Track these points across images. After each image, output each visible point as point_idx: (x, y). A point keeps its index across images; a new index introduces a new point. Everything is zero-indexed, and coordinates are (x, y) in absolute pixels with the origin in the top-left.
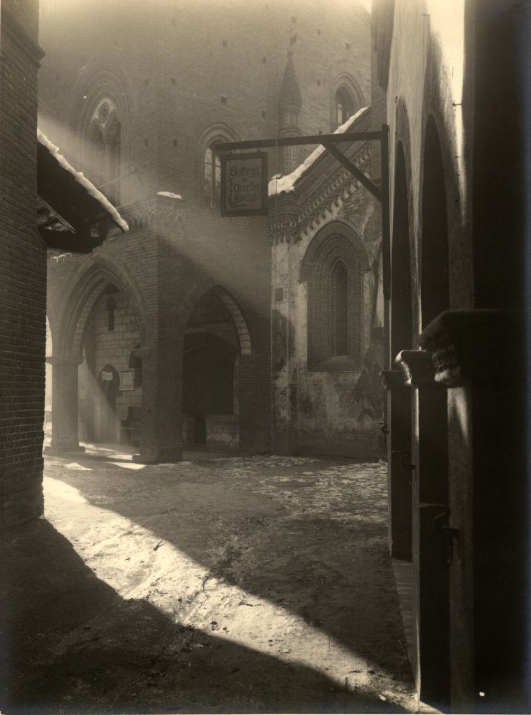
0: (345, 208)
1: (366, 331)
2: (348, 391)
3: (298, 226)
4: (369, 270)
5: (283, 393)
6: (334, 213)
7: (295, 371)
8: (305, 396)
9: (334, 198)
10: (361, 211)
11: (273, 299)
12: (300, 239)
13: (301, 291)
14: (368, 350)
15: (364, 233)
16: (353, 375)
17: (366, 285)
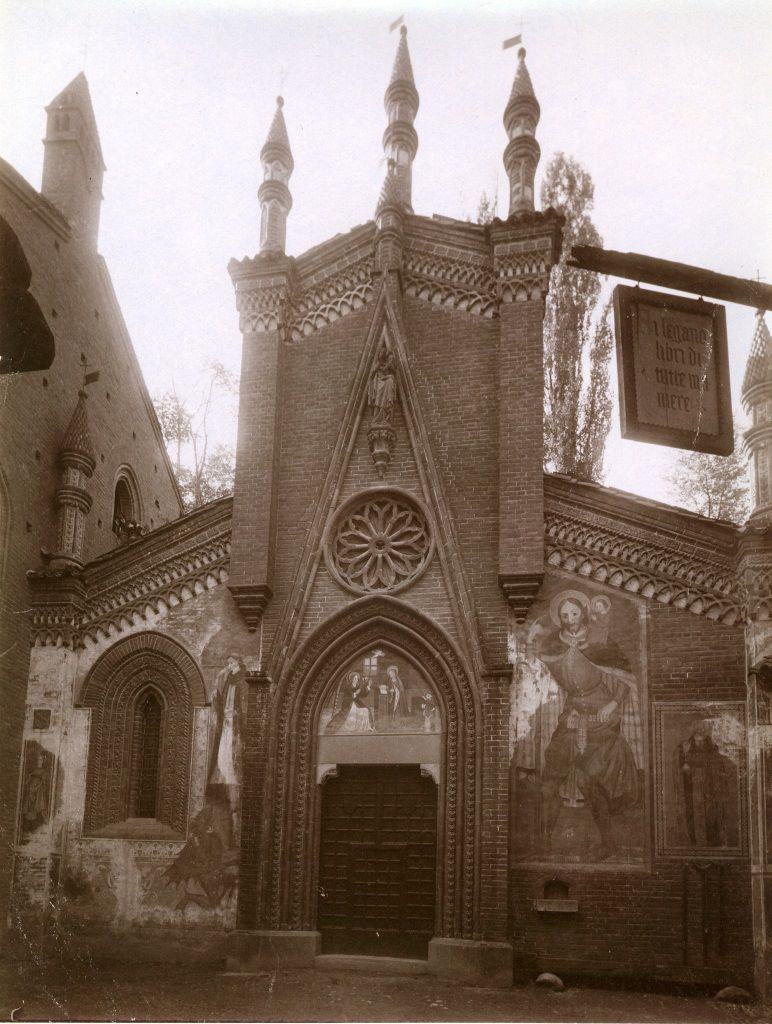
0: (170, 618)
1: (198, 787)
2: (159, 869)
3: (80, 629)
4: (208, 705)
5: (38, 866)
6: (152, 621)
7: (60, 836)
8: (74, 872)
9: (152, 600)
10: (199, 627)
11: (29, 723)
12: (83, 647)
13: (82, 721)
14: (200, 813)
15: (203, 655)
16: (171, 846)
17: (201, 724)
